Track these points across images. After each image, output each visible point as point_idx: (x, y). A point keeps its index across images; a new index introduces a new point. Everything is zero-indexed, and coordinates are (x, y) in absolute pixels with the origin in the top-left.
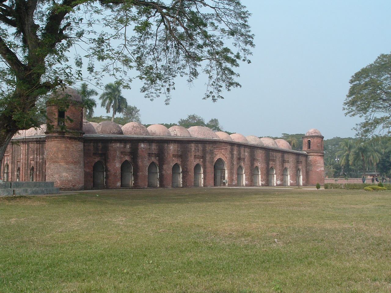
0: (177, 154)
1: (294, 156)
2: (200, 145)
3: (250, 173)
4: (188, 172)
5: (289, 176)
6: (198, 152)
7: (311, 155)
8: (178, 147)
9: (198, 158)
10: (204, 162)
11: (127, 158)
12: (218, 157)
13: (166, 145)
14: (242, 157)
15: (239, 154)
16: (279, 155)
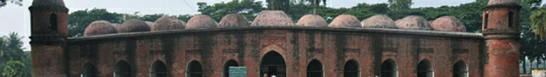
0: (193, 49)
1: (449, 42)
2: (232, 36)
3: (335, 70)
4: (212, 71)
5: (433, 73)
6: (229, 44)
7: (488, 39)
8: (195, 41)
9: (231, 52)
10: (241, 56)
11: (124, 58)
12: (268, 49)
13: (176, 39)
14: (316, 46)
15: (312, 43)
16: (409, 40)
